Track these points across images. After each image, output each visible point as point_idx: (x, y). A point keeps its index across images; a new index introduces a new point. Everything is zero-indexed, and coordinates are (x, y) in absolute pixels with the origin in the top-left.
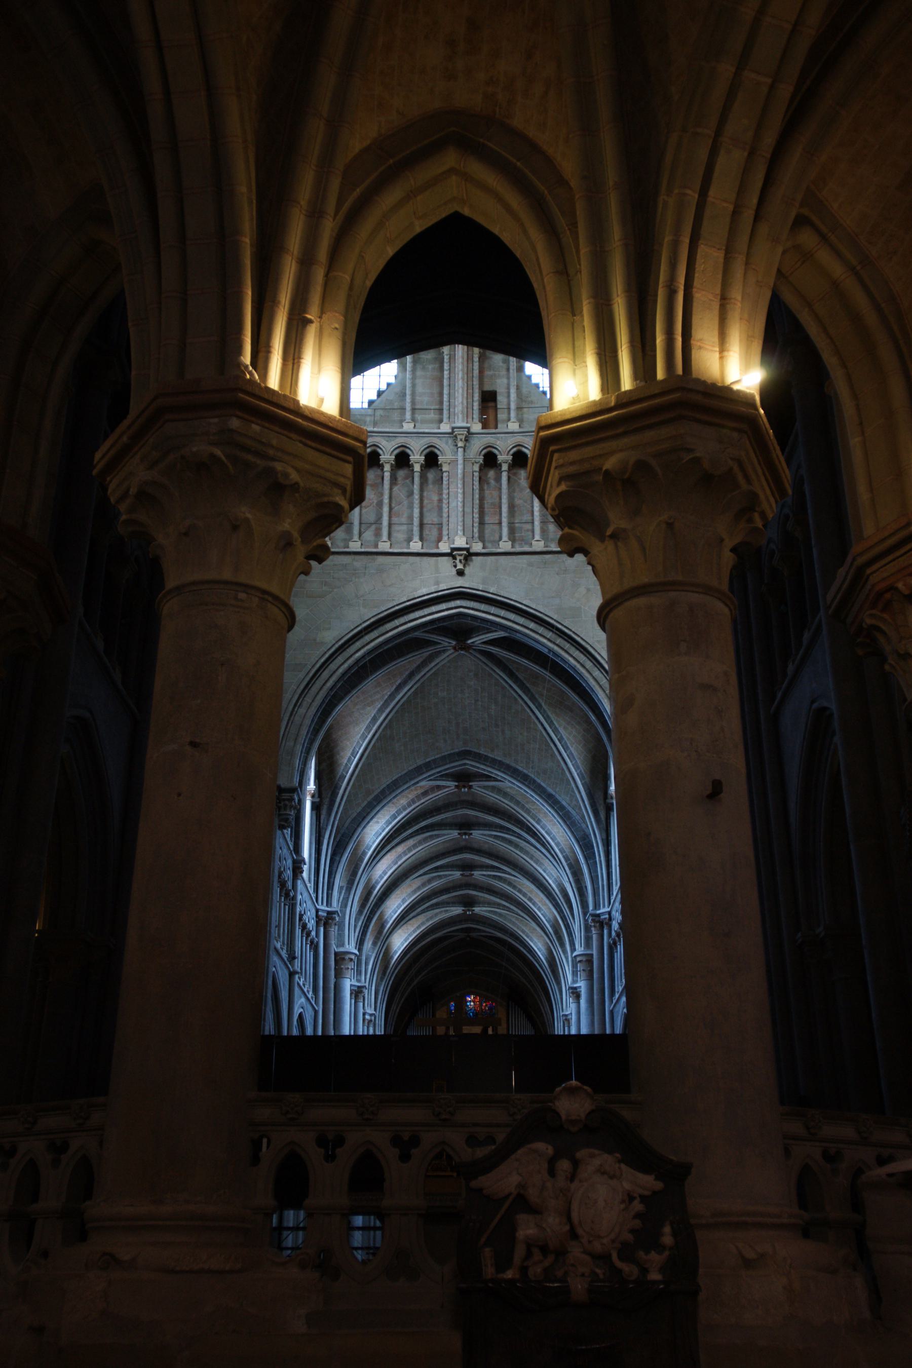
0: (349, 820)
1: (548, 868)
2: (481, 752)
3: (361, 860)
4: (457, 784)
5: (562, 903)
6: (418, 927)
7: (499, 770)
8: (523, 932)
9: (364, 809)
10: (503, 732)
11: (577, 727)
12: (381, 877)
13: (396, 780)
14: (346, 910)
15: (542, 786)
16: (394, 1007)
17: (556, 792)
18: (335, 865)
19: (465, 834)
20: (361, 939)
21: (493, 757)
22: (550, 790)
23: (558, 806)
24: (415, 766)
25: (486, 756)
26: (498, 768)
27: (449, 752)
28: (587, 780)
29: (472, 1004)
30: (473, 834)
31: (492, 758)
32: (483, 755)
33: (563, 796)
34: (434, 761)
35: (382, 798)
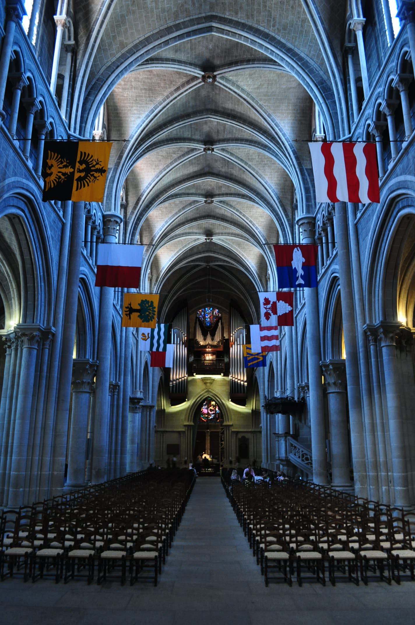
0: (104, 68)
1: (269, 181)
2: (226, 16)
4: (203, 73)
5: (278, 207)
6: (177, 252)
7: (243, 31)
8: (243, 255)
9: (118, 59)
12: (147, 188)
13: (149, 37)
14: (113, 185)
15: (282, 43)
16: (164, 308)
17: (295, 46)
18: (89, 104)
19: (209, 149)
20: (133, 232)
21: (237, 20)
22: (289, 45)
23: (297, 57)
24: (166, 26)
25: (230, 19)
26: (242, 29)
27: (197, 17)
28: (327, 27)
29: (209, 319)
30: (215, 150)
31: (236, 21)
32: (227, 19)
33: (301, 49)
34: (183, 23)
35: (135, 51)
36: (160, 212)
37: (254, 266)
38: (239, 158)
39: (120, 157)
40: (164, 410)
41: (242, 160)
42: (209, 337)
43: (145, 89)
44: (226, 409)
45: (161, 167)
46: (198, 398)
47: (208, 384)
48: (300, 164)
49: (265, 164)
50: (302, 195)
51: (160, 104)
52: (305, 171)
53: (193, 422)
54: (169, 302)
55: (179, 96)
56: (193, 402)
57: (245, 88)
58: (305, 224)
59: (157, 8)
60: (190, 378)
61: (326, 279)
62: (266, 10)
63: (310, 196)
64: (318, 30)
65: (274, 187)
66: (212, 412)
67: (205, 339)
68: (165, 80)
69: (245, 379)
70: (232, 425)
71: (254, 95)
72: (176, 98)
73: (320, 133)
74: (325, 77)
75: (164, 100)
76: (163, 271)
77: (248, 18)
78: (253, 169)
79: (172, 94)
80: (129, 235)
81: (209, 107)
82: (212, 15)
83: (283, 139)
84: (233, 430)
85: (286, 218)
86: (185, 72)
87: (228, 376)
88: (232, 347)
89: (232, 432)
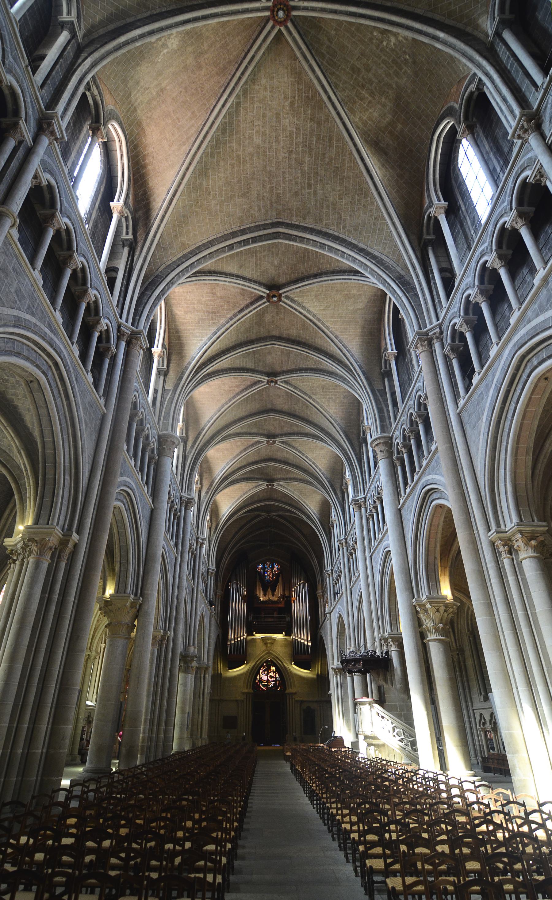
2: (293, 222)
3: (187, 368)
4: (268, 292)
8: (304, 502)
10: (315, 193)
11: (391, 171)
12: (209, 422)
13: (213, 240)
15: (353, 243)
16: (223, 561)
19: (272, 382)
21: (304, 225)
22: (361, 245)
24: (231, 231)
32: (295, 224)
34: (249, 228)
36: (221, 453)
37: (317, 513)
38: (303, 392)
39: (180, 379)
40: (221, 674)
41: (305, 394)
42: (269, 593)
43: (208, 312)
44: (288, 673)
45: (223, 402)
46: (257, 661)
47: (269, 645)
48: (370, 385)
49: (329, 398)
50: (375, 415)
51: (224, 325)
52: (377, 392)
53: (253, 689)
54: (229, 554)
55: (242, 317)
56: (252, 665)
57: (311, 309)
58: (381, 444)
59: (222, 212)
60: (250, 638)
61: (414, 497)
62: (335, 212)
63: (384, 416)
64: (394, 224)
65: (339, 421)
66: (272, 679)
67: (265, 595)
68: (228, 302)
69: (309, 639)
70: (296, 693)
71: (320, 317)
72: (240, 319)
73: (392, 350)
74: (403, 273)
75: (228, 322)
76: (223, 519)
77: (317, 222)
78: (318, 403)
79: (235, 315)
80: (188, 469)
81: (274, 333)
82: (278, 222)
83: (352, 360)
84: (297, 699)
85: (353, 451)
86: (250, 289)
87: (290, 636)
88: (294, 603)
89: (296, 701)
